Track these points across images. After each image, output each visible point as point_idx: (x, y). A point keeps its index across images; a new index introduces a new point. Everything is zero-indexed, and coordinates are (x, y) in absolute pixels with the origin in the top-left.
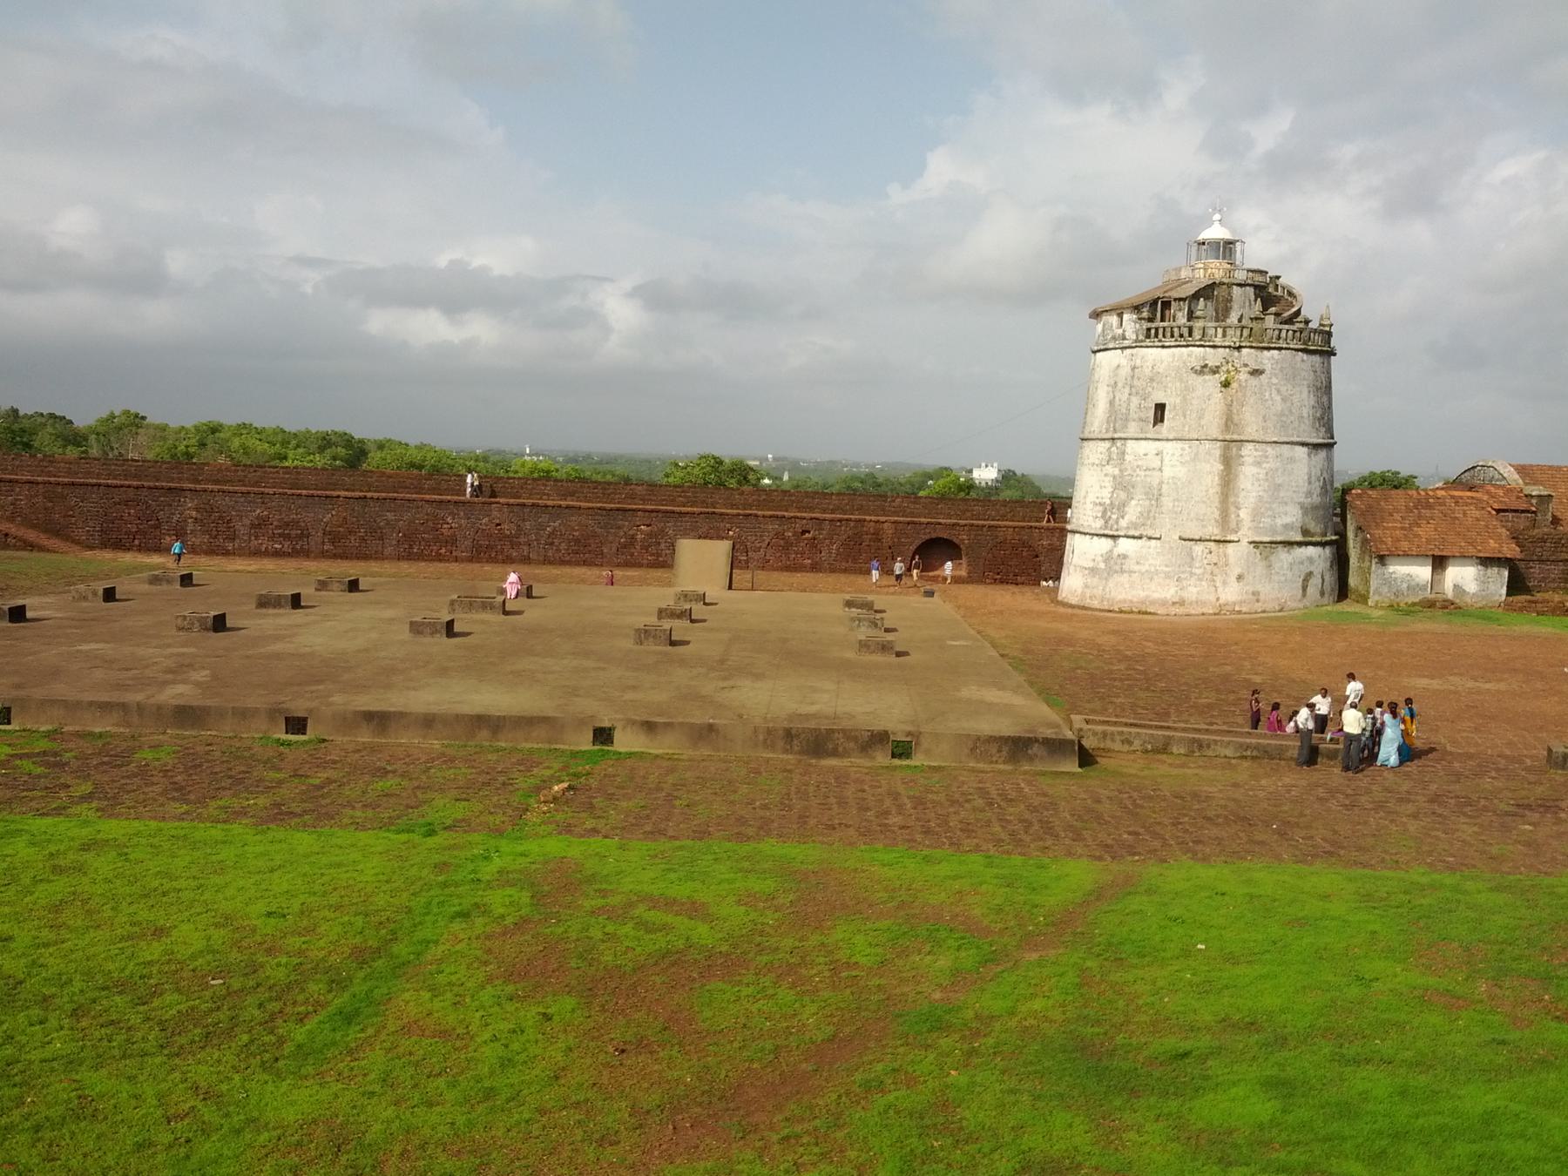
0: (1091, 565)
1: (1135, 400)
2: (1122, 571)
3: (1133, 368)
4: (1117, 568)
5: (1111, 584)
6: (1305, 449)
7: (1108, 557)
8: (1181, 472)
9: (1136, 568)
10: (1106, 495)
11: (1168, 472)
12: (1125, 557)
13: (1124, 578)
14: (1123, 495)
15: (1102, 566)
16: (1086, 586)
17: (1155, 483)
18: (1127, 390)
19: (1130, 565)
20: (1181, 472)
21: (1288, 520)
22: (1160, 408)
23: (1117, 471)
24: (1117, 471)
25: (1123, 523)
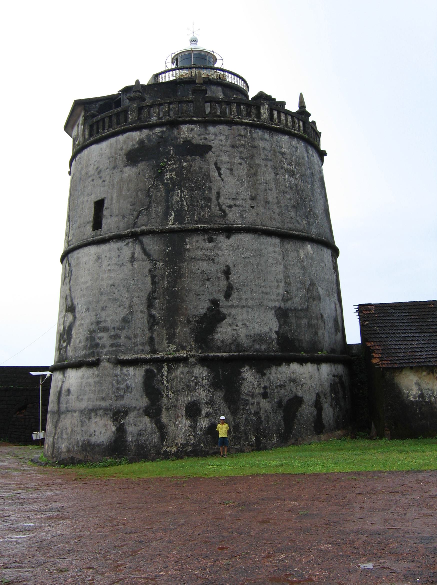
6: (277, 241)
14: (70, 317)
21: (257, 329)
22: (99, 205)
24: (68, 292)
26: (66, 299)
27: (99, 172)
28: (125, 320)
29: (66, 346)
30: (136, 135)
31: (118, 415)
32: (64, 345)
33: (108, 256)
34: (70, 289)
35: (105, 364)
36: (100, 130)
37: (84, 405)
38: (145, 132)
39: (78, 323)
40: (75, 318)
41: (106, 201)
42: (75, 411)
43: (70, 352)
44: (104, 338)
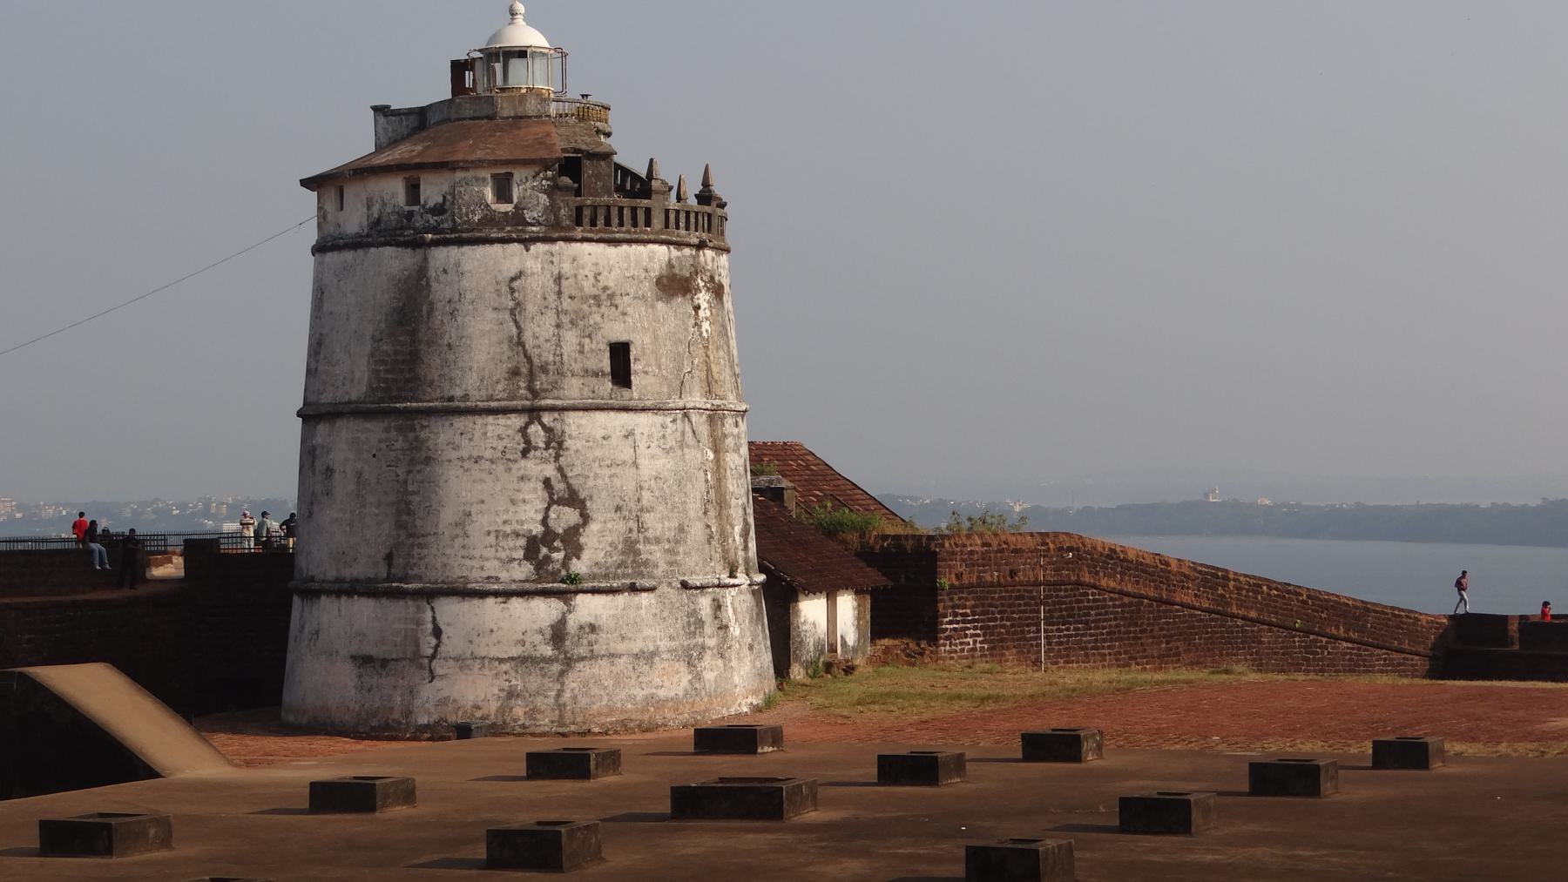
0: (516, 651)
1: (571, 338)
2: (593, 657)
3: (558, 279)
4: (583, 651)
5: (572, 682)
7: (558, 634)
8: (664, 464)
9: (622, 647)
10: (529, 517)
11: (648, 468)
12: (593, 628)
13: (601, 669)
14: (570, 516)
15: (548, 651)
16: (512, 694)
17: (630, 487)
18: (550, 318)
19: (603, 644)
20: (664, 464)
23: (550, 471)
24: (550, 471)
25: (579, 566)
26: (547, 483)
27: (611, 297)
28: (681, 529)
29: (567, 559)
30: (662, 250)
31: (691, 656)
32: (558, 556)
33: (646, 432)
34: (560, 469)
35: (664, 588)
36: (601, 221)
37: (636, 646)
38: (675, 253)
39: (594, 527)
40: (586, 519)
41: (632, 348)
42: (620, 656)
43: (579, 566)
44: (655, 554)
